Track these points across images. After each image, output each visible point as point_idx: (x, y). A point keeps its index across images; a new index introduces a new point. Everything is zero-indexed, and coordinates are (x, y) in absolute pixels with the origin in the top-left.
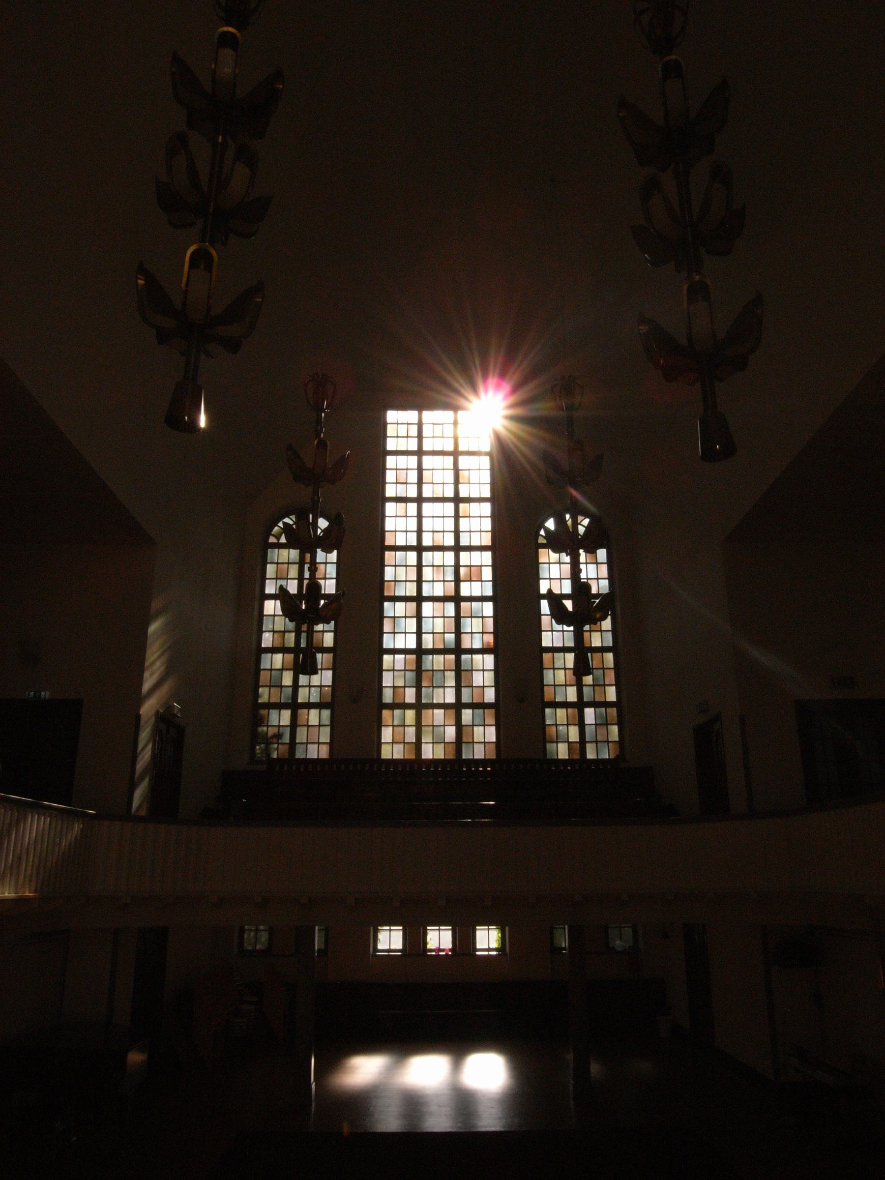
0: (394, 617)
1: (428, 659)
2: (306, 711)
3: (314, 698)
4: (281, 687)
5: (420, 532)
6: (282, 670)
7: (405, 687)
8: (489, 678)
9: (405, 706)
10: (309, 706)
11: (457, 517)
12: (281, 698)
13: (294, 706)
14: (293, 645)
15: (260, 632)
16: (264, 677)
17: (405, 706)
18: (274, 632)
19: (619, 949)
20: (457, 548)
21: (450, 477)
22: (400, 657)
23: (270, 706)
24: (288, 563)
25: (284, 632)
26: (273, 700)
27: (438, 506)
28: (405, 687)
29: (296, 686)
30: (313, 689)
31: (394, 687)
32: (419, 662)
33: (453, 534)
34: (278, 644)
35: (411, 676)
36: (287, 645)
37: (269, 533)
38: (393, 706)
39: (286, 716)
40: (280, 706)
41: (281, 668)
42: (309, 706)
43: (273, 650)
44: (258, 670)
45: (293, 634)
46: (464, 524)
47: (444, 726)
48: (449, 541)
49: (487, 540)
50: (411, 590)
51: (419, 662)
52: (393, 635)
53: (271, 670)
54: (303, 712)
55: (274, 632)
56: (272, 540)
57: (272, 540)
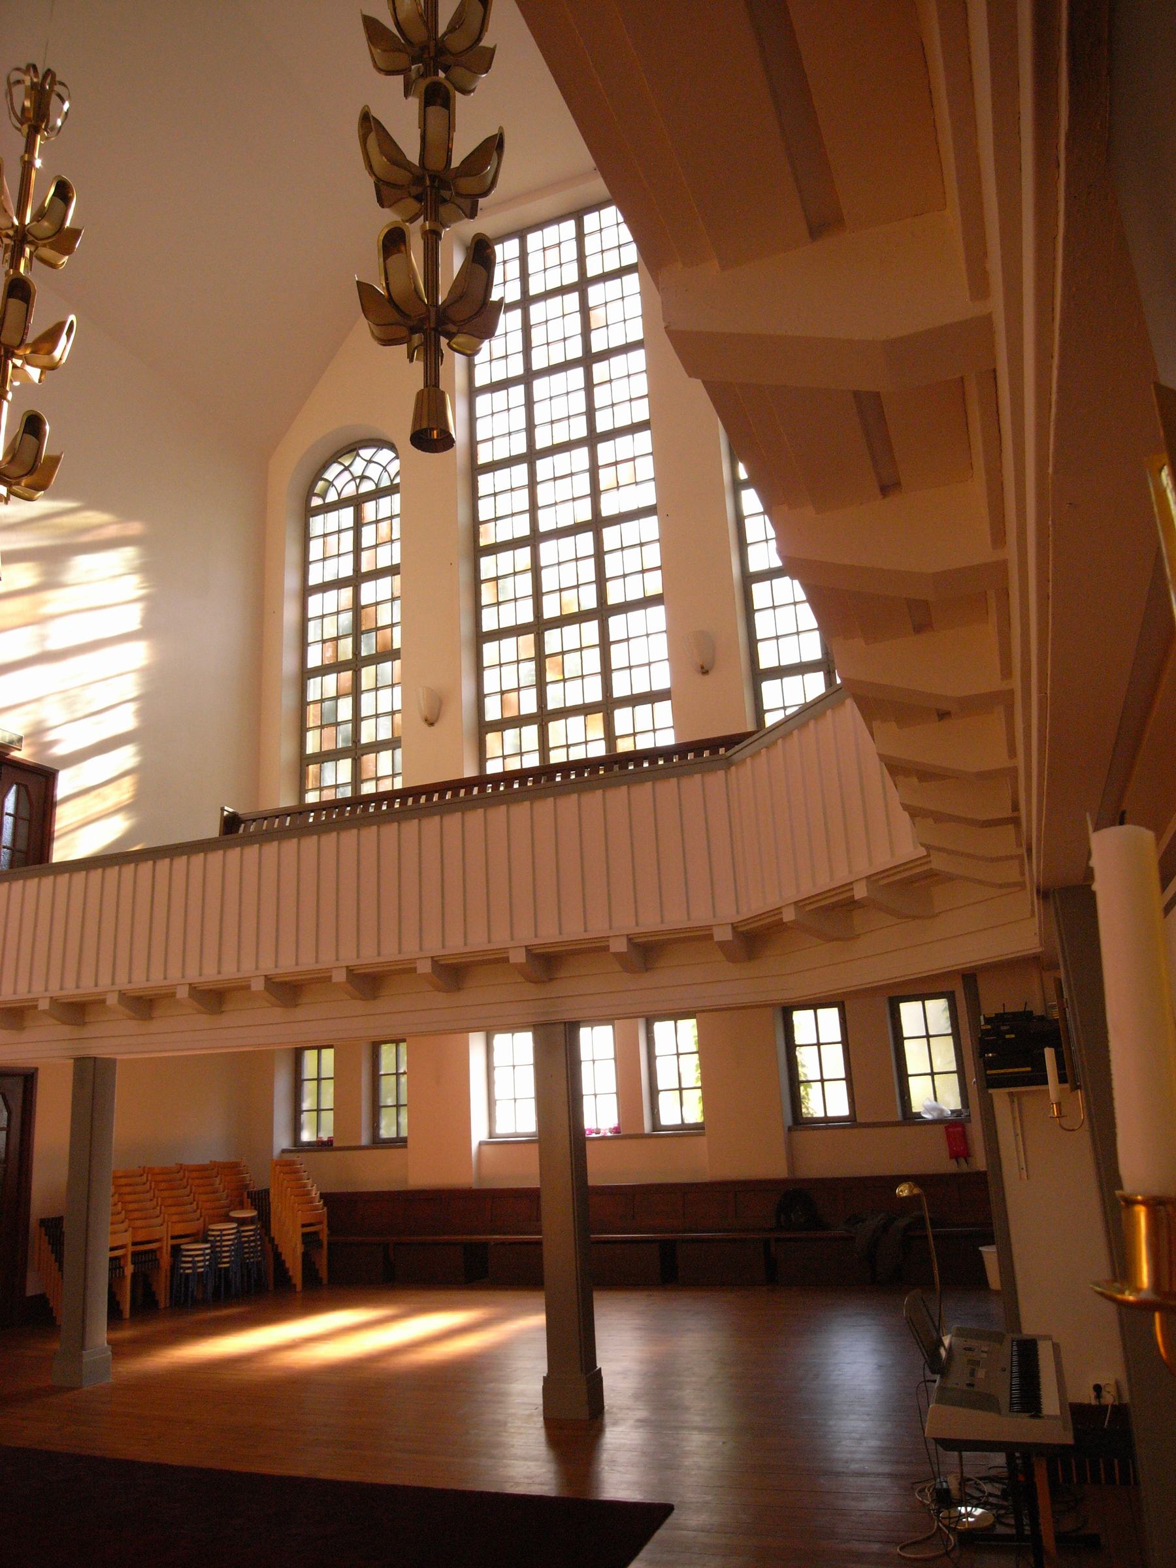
1: (553, 640)
3: (385, 734)
6: (336, 698)
7: (518, 689)
8: (660, 647)
9: (519, 721)
10: (377, 747)
11: (589, 386)
15: (304, 644)
16: (313, 716)
17: (519, 721)
18: (324, 641)
19: (928, 1116)
20: (593, 439)
22: (509, 644)
23: (323, 757)
25: (336, 639)
27: (558, 378)
28: (518, 689)
29: (357, 719)
30: (381, 720)
31: (502, 693)
32: (539, 644)
35: (528, 671)
36: (342, 658)
37: (310, 494)
38: (501, 725)
39: (345, 765)
40: (334, 755)
41: (335, 695)
42: (377, 747)
43: (323, 671)
44: (303, 704)
45: (350, 640)
47: (586, 742)
51: (539, 644)
53: (322, 701)
54: (368, 759)
56: (316, 502)
57: (316, 502)
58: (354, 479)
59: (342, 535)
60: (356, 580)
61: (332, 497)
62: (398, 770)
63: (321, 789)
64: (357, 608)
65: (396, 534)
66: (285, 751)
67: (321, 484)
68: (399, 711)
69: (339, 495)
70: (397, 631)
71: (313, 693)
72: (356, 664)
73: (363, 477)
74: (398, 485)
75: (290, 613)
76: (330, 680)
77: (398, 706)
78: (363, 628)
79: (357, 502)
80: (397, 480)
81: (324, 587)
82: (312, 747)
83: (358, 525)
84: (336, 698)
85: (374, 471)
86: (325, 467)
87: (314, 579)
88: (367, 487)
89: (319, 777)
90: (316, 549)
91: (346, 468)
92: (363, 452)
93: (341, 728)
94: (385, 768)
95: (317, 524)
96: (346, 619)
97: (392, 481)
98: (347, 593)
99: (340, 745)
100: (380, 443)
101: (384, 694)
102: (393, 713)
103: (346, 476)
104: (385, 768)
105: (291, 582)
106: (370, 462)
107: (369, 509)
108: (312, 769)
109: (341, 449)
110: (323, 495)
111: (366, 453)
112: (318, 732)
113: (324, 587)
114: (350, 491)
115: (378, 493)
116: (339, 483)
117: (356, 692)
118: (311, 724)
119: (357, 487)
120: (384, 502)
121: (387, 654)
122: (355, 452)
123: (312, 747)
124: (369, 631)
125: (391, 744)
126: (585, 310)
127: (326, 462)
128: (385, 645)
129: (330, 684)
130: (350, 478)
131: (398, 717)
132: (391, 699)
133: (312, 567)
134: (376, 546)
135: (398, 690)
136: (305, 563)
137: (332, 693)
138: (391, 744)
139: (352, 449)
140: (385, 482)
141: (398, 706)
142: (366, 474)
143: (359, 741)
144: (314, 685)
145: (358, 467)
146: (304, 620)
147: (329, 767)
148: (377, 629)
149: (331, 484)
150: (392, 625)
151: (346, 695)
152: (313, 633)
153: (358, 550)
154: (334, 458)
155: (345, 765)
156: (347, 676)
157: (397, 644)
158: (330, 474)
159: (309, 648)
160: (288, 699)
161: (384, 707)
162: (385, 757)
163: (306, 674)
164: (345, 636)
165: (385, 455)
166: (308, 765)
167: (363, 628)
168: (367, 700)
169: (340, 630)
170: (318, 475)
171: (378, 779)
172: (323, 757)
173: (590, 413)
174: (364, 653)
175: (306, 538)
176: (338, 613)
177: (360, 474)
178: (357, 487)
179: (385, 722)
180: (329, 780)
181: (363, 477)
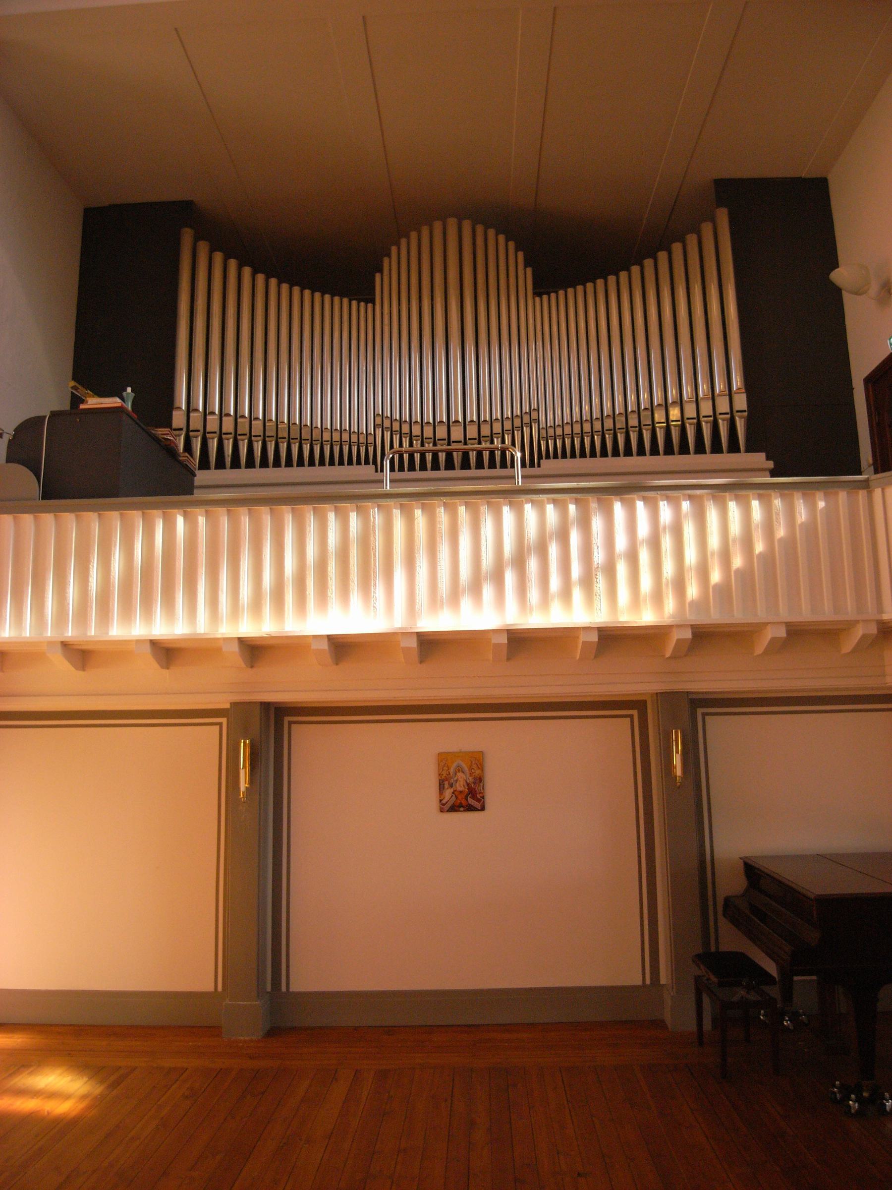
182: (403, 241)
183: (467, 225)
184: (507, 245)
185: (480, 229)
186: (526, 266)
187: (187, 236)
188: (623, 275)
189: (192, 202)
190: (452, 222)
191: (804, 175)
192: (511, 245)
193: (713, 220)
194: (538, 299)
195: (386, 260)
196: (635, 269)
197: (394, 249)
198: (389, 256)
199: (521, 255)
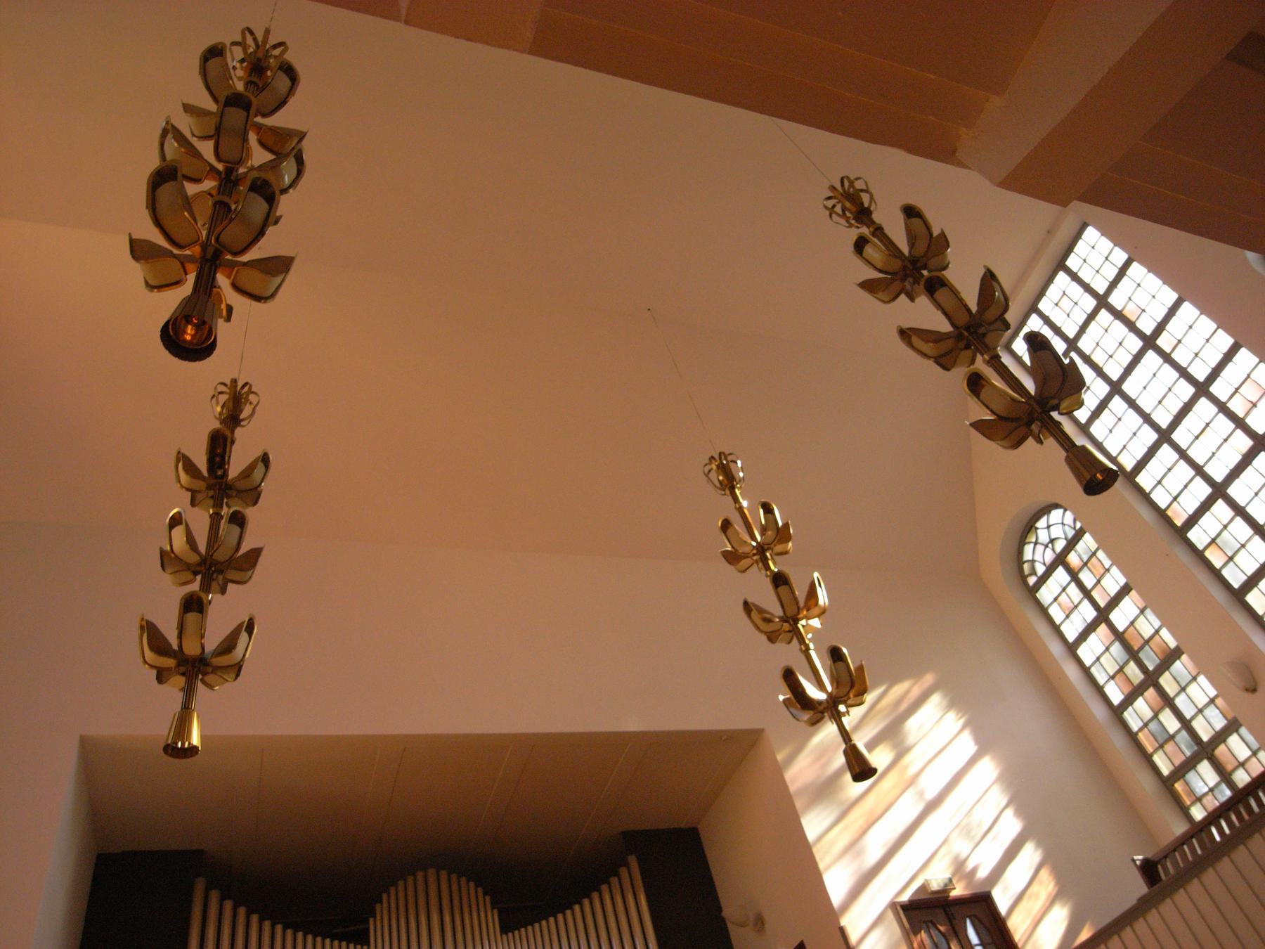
0: (1213, 541)
2: (1222, 747)
3: (1219, 723)
4: (1172, 737)
5: (1147, 419)
6: (1156, 716)
11: (1167, 358)
12: (1183, 753)
13: (1205, 750)
14: (1141, 676)
15: (1099, 690)
18: (1112, 677)
21: (1119, 328)
23: (1182, 770)
24: (1064, 589)
25: (1121, 670)
26: (1178, 760)
29: (1186, 724)
30: (1207, 712)
33: (1182, 380)
34: (1127, 690)
37: (1024, 578)
40: (1189, 765)
42: (1220, 737)
43: (1129, 700)
44: (1132, 736)
45: (1132, 664)
46: (1181, 357)
48: (1187, 390)
49: (1224, 341)
50: (1201, 490)
52: (1231, 563)
53: (1146, 725)
54: (1221, 751)
55: (1112, 677)
56: (1032, 580)
57: (1032, 580)
58: (1046, 546)
59: (1068, 590)
60: (1103, 615)
61: (1040, 569)
62: (1255, 745)
63: (1199, 799)
64: (1119, 636)
65: (1107, 563)
66: (1147, 783)
67: (1026, 567)
68: (1216, 696)
69: (1044, 564)
70: (1165, 633)
71: (1135, 725)
72: (1151, 679)
73: (1052, 541)
74: (1081, 528)
75: (1072, 672)
76: (1140, 704)
77: (1212, 692)
78: (1136, 648)
79: (1060, 560)
80: (1078, 525)
81: (1083, 636)
82: (1165, 770)
83: (1074, 575)
84: (1156, 716)
85: (1057, 532)
86: (1020, 552)
87: (1071, 636)
88: (1060, 545)
89: (1191, 791)
90: (1056, 614)
91: (1036, 543)
92: (1039, 525)
93: (1178, 738)
94: (1243, 752)
95: (1046, 594)
96: (1117, 648)
97: (1074, 528)
98: (1103, 628)
99: (1188, 753)
100: (1046, 510)
101: (1193, 689)
102: (1212, 701)
103: (1040, 548)
104: (1243, 752)
105: (1056, 649)
106: (1049, 527)
107: (1073, 559)
108: (1179, 786)
109: (1023, 533)
110: (1033, 572)
111: (1042, 523)
112: (1160, 752)
113: (1083, 636)
114: (1049, 556)
115: (1072, 544)
116: (1038, 557)
117: (1168, 702)
118: (1150, 749)
119: (1053, 550)
120: (1080, 546)
121: (1171, 657)
122: (1033, 529)
123: (1165, 770)
124: (1142, 648)
125: (1232, 727)
126: (1118, 315)
127: (1019, 548)
128: (1164, 652)
129: (1142, 707)
130: (1043, 547)
131: (1219, 701)
132: (1202, 690)
133: (1062, 628)
134: (1099, 581)
135: (1202, 679)
136: (1056, 629)
137: (1148, 714)
138: (1232, 727)
139: (1030, 527)
140: (1071, 533)
141: (1212, 692)
142: (1053, 537)
143: (1201, 740)
144: (1129, 715)
145: (1043, 536)
146: (1086, 671)
147: (1191, 776)
148: (1147, 642)
149: (1033, 561)
150: (1157, 632)
151: (1161, 709)
152: (1101, 678)
153: (1087, 593)
154: (1022, 543)
155: (1205, 767)
156: (1151, 692)
157: (1172, 644)
158: (1028, 552)
159: (1105, 689)
160: (1118, 740)
161: (1202, 700)
162: (1234, 740)
163: (1117, 712)
164: (1126, 663)
165: (1056, 515)
166: (1173, 785)
167: (1136, 648)
168: (1180, 702)
169: (1119, 660)
170: (1020, 561)
171: (1242, 764)
172: (1182, 770)
173: (1184, 373)
174: (1151, 668)
175: (1043, 611)
176: (1107, 649)
177: (1048, 540)
178: (1053, 550)
179: (1212, 712)
180: (1201, 788)
181: (1052, 541)
182: (392, 890)
183: (444, 874)
184: (459, 881)
185: (454, 877)
186: (493, 908)
187: (200, 885)
188: (568, 912)
189: (202, 851)
190: (431, 872)
191: (682, 826)
192: (480, 890)
193: (626, 865)
194: (504, 936)
195: (378, 906)
196: (577, 907)
197: (385, 896)
198: (381, 902)
199: (488, 898)
